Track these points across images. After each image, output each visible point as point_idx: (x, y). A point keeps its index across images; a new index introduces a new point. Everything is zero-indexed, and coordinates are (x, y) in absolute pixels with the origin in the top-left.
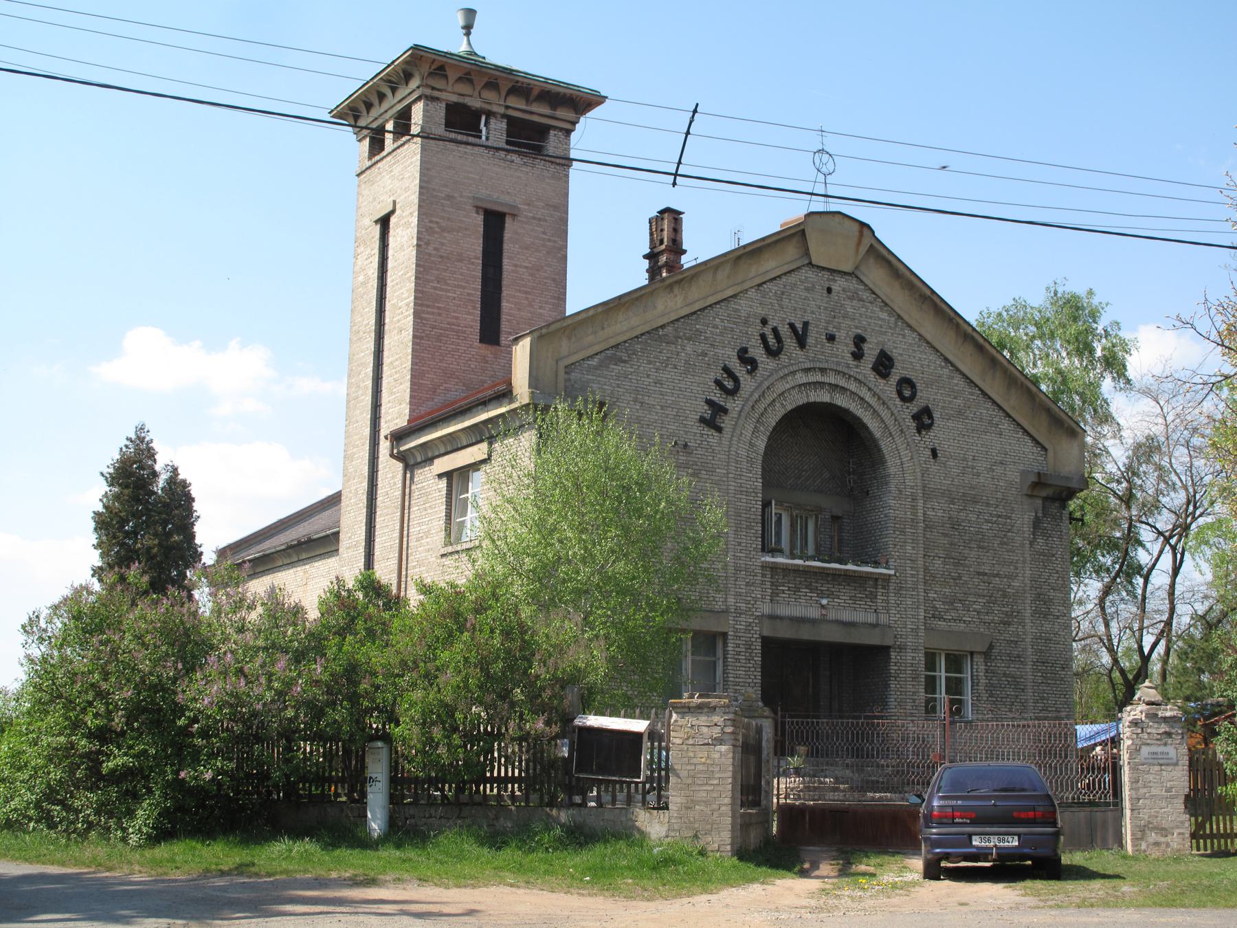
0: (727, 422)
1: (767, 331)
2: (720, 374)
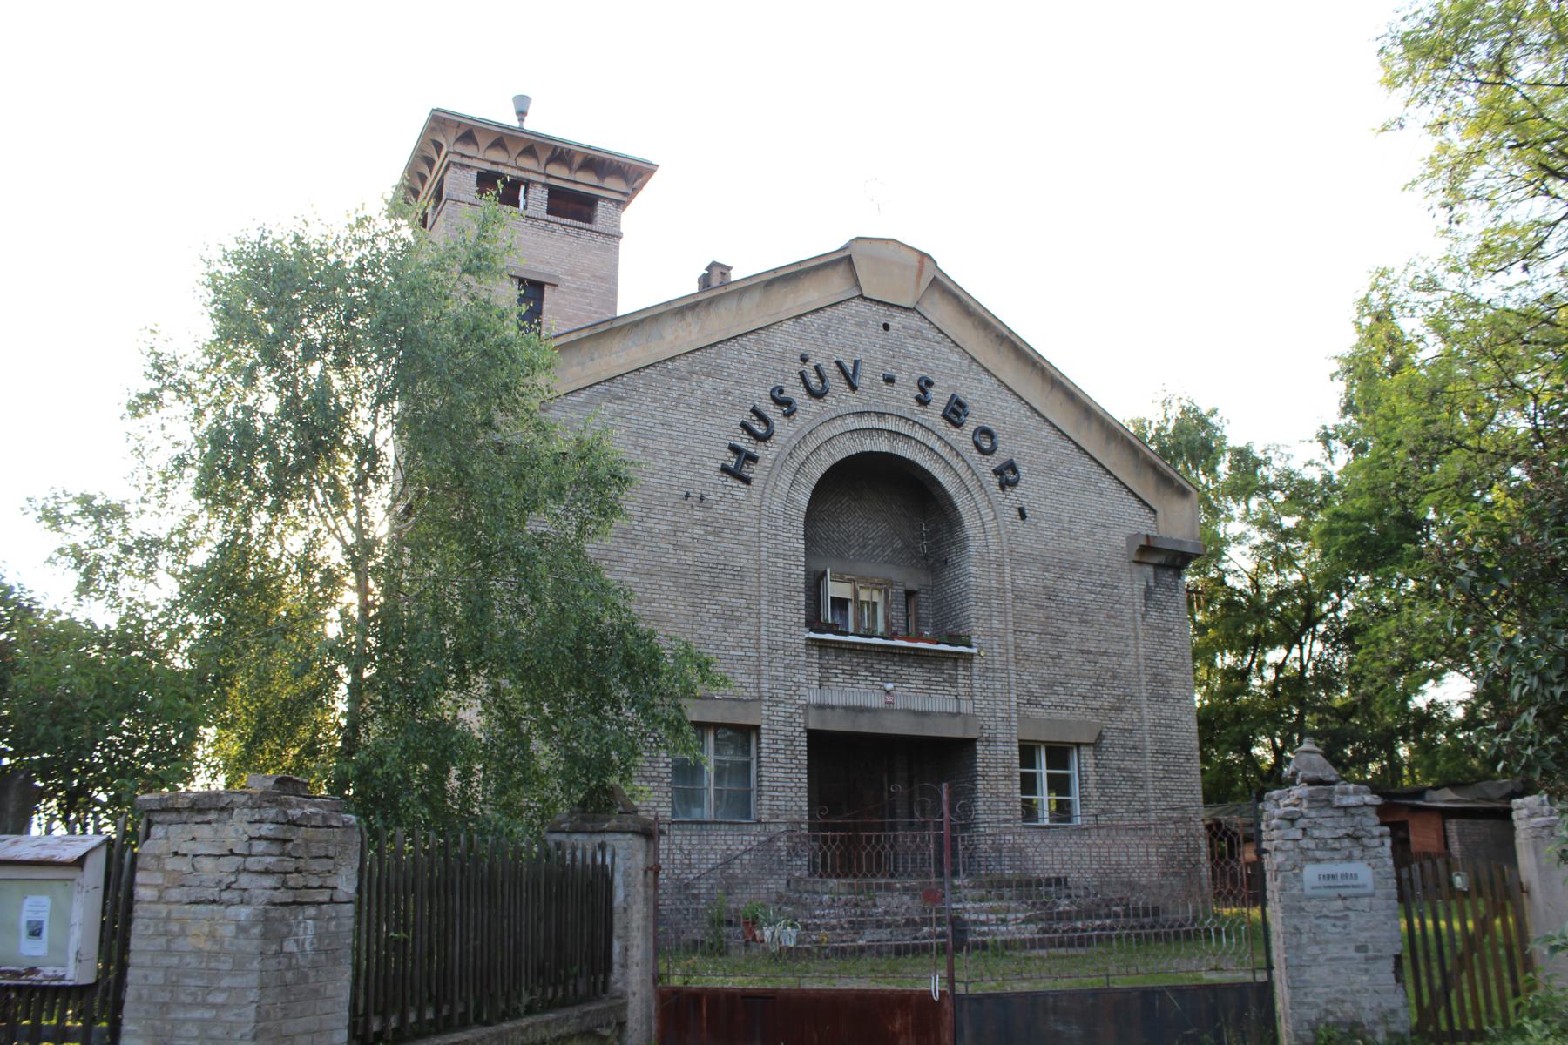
0: (756, 472)
1: (809, 369)
2: (748, 417)
